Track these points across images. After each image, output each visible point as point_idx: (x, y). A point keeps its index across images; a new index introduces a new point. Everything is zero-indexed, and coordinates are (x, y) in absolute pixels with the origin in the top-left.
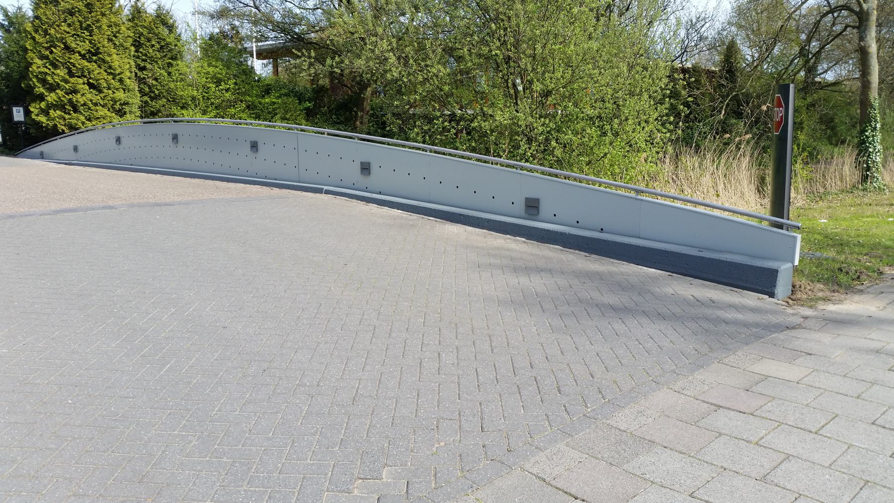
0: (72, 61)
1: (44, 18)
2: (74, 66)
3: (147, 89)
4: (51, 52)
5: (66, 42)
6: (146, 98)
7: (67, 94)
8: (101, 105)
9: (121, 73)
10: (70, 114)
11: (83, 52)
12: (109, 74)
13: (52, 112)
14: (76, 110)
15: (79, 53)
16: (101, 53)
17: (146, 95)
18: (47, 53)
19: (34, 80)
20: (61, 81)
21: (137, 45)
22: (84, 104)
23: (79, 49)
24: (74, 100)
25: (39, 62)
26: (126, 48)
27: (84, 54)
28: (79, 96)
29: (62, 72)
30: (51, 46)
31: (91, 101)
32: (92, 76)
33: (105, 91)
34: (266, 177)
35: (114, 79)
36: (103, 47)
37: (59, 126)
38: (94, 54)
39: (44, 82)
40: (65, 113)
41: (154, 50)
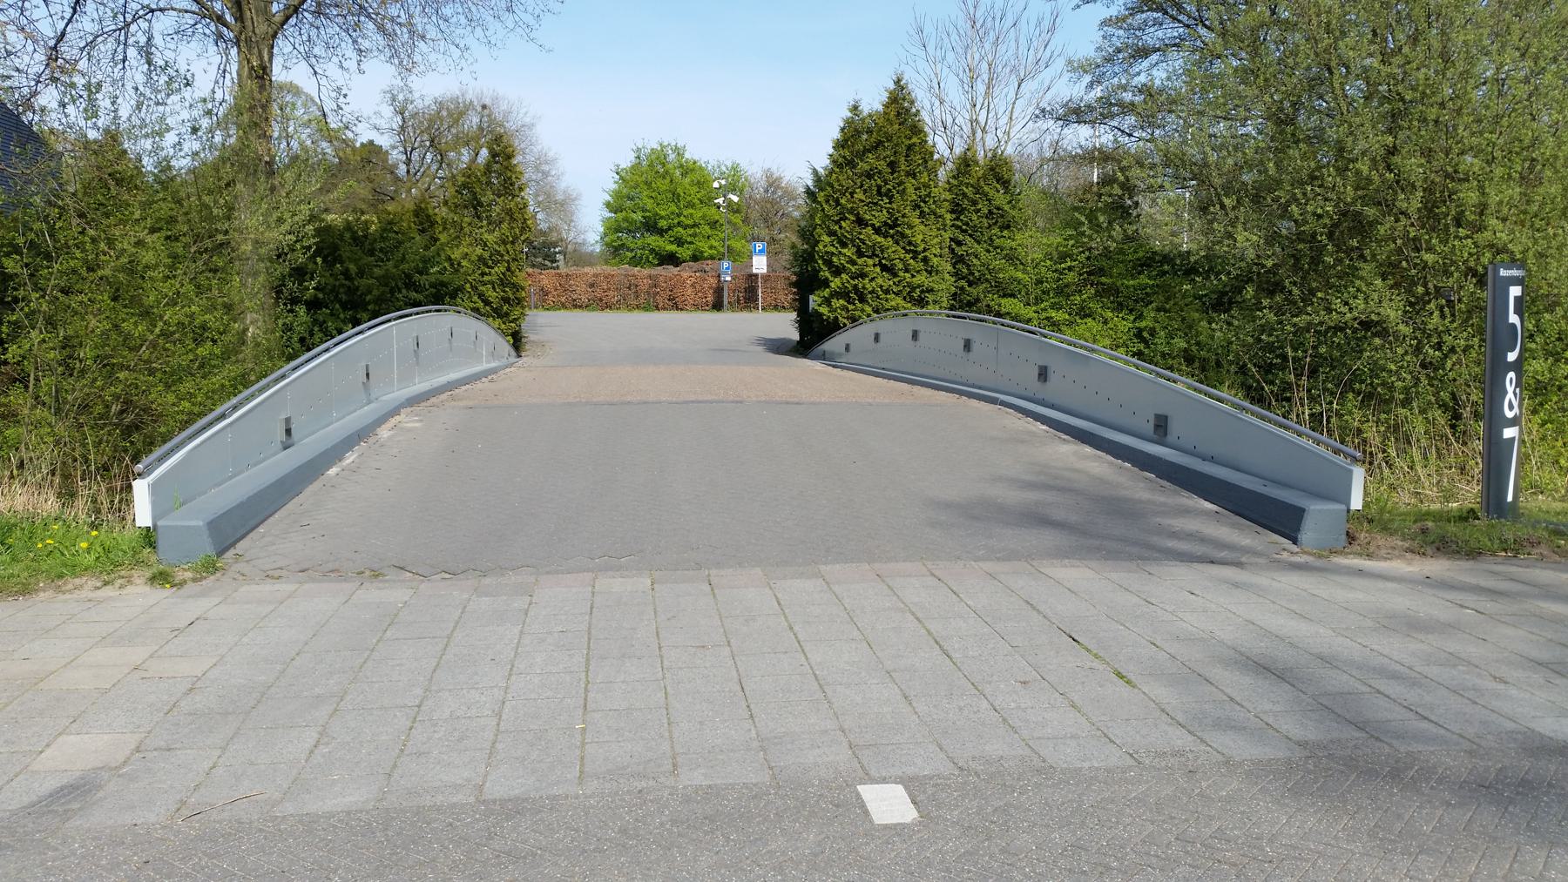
0: (862, 237)
1: (836, 185)
2: (864, 244)
3: (965, 271)
4: (841, 227)
5: (858, 213)
6: (963, 283)
7: (853, 278)
8: (894, 293)
9: (925, 250)
10: (854, 304)
11: (877, 225)
12: (908, 252)
13: (834, 301)
14: (862, 300)
15: (873, 225)
16: (899, 225)
17: (963, 278)
18: (837, 227)
19: (820, 262)
20: (847, 262)
21: (957, 210)
22: (872, 292)
23: (875, 222)
24: (860, 286)
25: (826, 239)
26: (940, 217)
27: (880, 227)
28: (867, 281)
29: (849, 252)
30: (841, 219)
31: (881, 287)
32: (886, 256)
33: (901, 274)
34: (973, 386)
35: (914, 258)
36: (903, 216)
37: (840, 318)
38: (891, 228)
39: (829, 263)
40: (849, 303)
41: (979, 217)
